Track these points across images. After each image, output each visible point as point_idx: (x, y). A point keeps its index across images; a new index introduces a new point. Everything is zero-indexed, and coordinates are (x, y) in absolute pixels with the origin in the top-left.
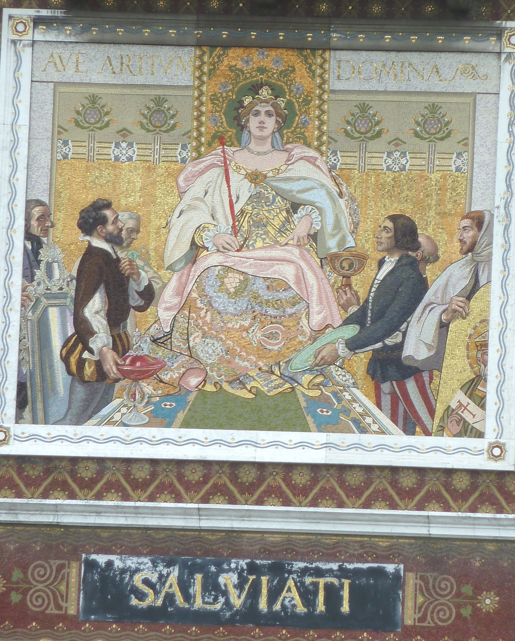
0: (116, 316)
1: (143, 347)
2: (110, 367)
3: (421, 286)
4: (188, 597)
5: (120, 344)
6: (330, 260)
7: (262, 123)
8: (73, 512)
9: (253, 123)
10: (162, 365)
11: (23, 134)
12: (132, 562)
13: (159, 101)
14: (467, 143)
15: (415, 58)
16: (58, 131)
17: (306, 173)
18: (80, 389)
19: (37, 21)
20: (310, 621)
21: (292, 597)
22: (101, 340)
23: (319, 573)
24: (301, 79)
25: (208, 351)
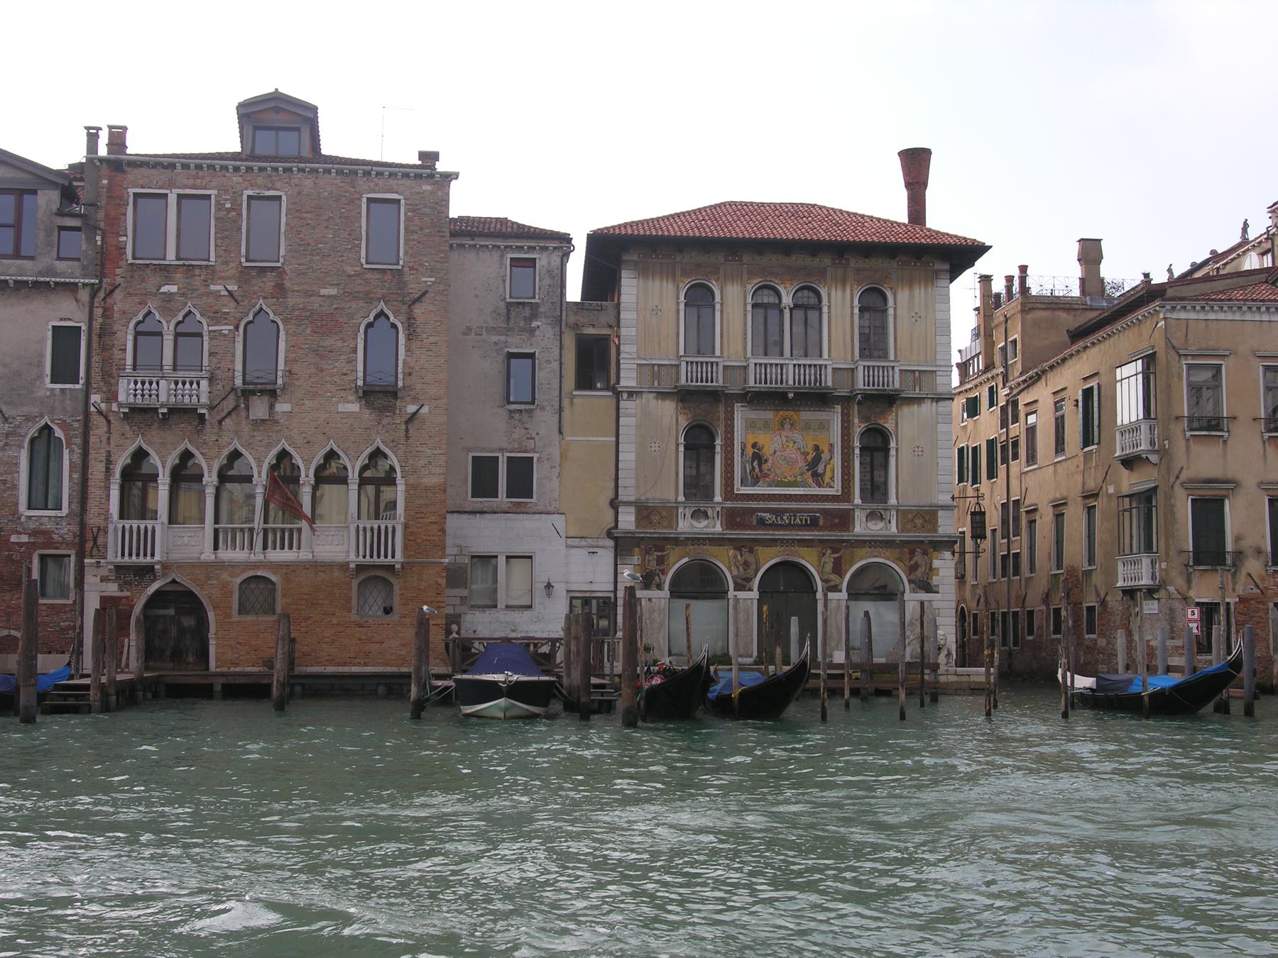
0: (760, 465)
5: (761, 471)
7: (787, 426)
8: (754, 505)
17: (797, 436)
20: (801, 525)
22: (757, 470)
25: (779, 472)
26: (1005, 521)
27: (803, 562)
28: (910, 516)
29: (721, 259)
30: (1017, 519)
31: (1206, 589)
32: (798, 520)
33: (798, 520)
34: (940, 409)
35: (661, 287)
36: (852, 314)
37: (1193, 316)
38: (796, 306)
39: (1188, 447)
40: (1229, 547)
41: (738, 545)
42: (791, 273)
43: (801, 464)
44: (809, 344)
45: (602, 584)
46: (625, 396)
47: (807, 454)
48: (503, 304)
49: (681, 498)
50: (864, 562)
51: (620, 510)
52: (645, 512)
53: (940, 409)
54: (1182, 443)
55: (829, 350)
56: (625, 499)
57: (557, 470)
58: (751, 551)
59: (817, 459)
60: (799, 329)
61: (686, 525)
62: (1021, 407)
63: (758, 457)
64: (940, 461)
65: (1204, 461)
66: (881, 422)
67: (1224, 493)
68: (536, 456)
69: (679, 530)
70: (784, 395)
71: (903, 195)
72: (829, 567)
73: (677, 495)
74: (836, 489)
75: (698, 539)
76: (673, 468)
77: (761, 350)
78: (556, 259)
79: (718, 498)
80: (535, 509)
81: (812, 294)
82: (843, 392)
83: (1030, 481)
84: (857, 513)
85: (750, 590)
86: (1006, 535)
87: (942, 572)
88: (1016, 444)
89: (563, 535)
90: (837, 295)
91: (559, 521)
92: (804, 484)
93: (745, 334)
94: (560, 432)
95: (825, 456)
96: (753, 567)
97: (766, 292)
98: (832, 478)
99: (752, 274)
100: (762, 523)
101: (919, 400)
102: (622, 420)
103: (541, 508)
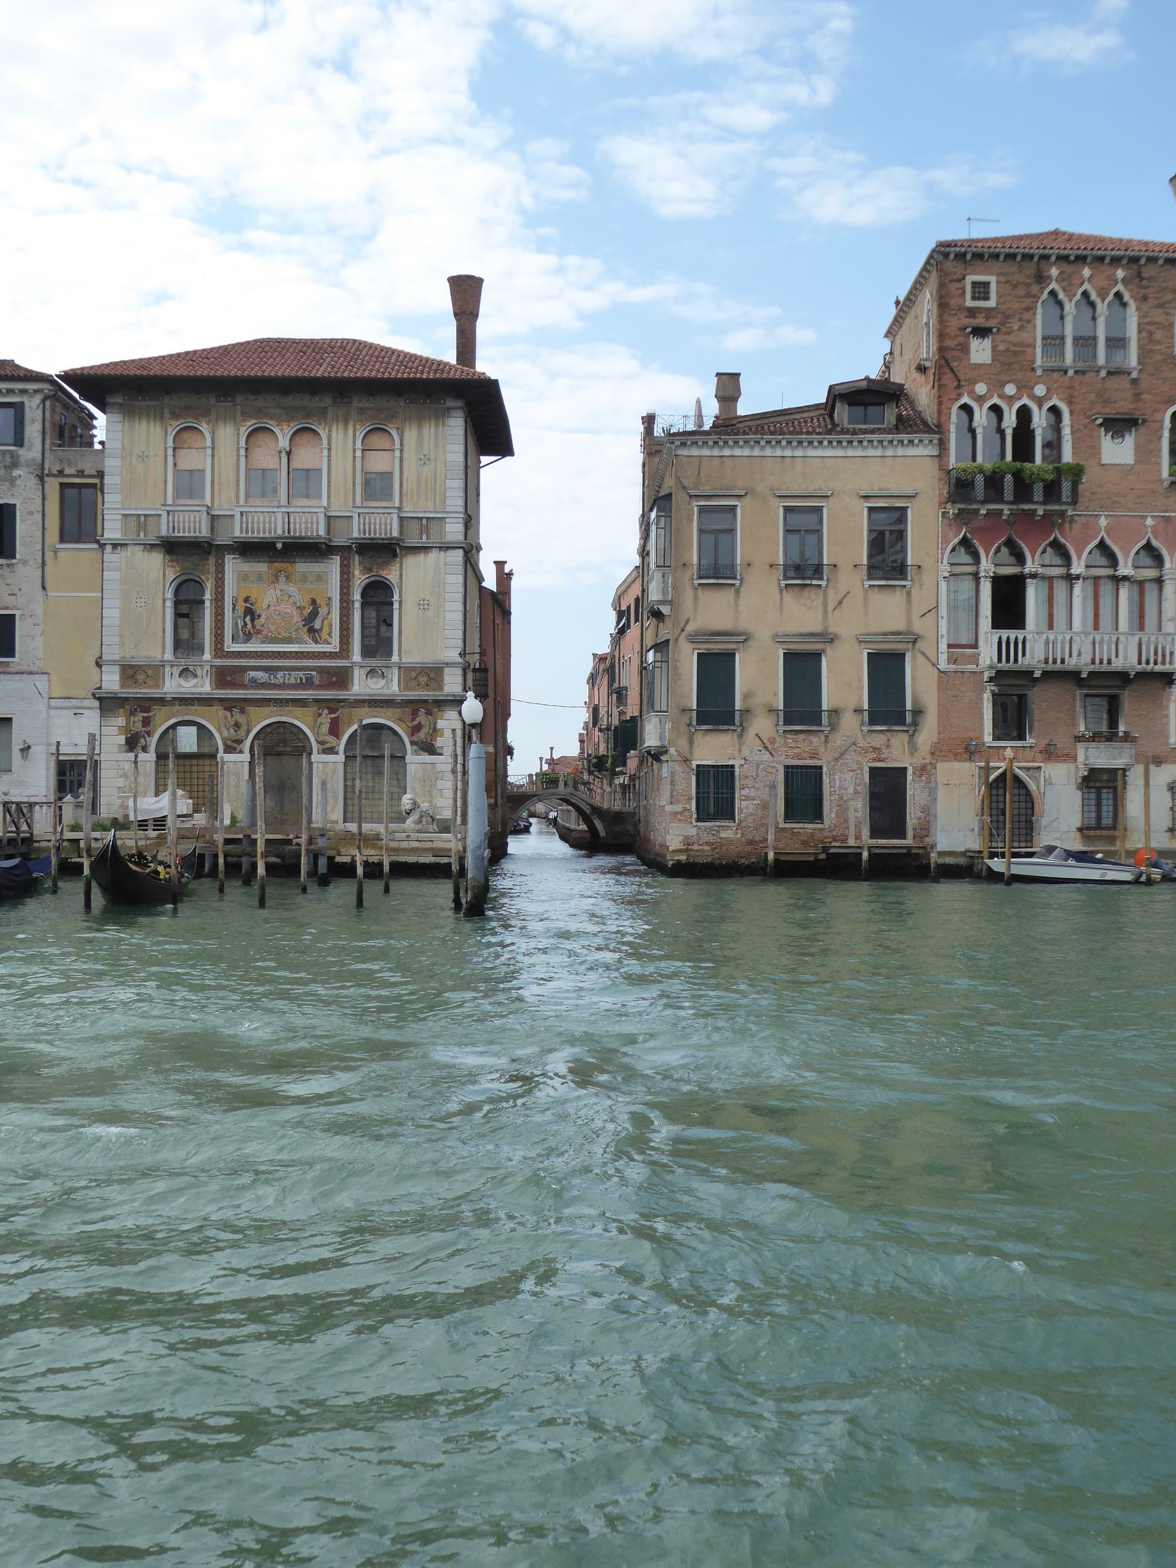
0: (252, 621)
1: (258, 627)
5: (254, 627)
7: (282, 579)
17: (292, 589)
21: (293, 681)
24: (290, 569)
25: (273, 628)
28: (414, 674)
29: (213, 400)
31: (713, 749)
34: (449, 559)
35: (148, 433)
36: (354, 457)
37: (706, 452)
39: (696, 597)
40: (909, 706)
41: (228, 704)
42: (289, 414)
43: (297, 619)
46: (109, 548)
47: (301, 608)
49: (169, 656)
52: (130, 672)
54: (689, 594)
55: (329, 496)
57: (39, 629)
58: (242, 711)
59: (314, 615)
61: (173, 685)
63: (249, 612)
65: (713, 611)
66: (384, 573)
67: (733, 646)
68: (17, 613)
69: (165, 690)
72: (325, 729)
73: (164, 653)
76: (160, 624)
79: (207, 656)
80: (17, 669)
82: (339, 541)
85: (241, 752)
89: (46, 696)
91: (41, 682)
93: (238, 481)
94: (44, 588)
95: (323, 611)
96: (244, 728)
98: (330, 634)
99: (246, 415)
100: (256, 685)
101: (425, 549)
103: (24, 668)
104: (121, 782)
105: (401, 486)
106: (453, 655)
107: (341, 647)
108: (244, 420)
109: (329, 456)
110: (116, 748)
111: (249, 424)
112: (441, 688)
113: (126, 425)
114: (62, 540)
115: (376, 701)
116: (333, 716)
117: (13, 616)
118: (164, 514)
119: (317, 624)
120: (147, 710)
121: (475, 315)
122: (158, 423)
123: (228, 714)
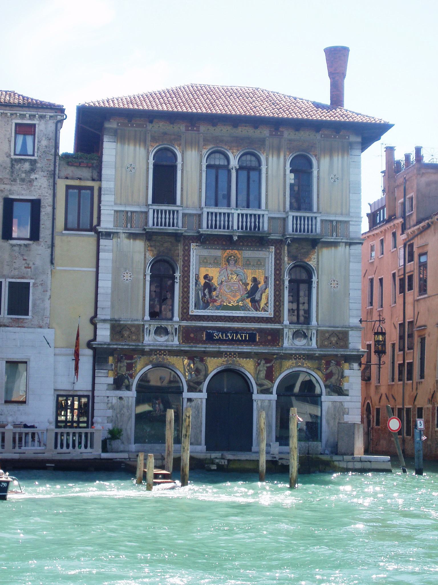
0: (210, 292)
2: (209, 301)
3: (258, 288)
4: (223, 337)
6: (243, 283)
9: (231, 262)
10: (217, 300)
11: (195, 263)
12: (214, 332)
13: (216, 258)
14: (264, 265)
15: (256, 252)
16: (200, 263)
18: (204, 305)
19: (196, 245)
20: (242, 341)
23: (243, 333)
26: (402, 338)
27: (243, 370)
28: (327, 335)
29: (183, 128)
30: (411, 336)
32: (239, 336)
33: (239, 336)
35: (135, 150)
38: (241, 168)
41: (192, 356)
42: (237, 142)
44: (251, 197)
45: (83, 384)
48: (8, 160)
49: (147, 317)
50: (291, 371)
51: (98, 326)
53: (352, 251)
56: (103, 317)
59: (255, 288)
60: (243, 185)
61: (150, 340)
62: (415, 249)
63: (209, 286)
64: (351, 292)
66: (306, 260)
68: (32, 282)
70: (231, 237)
71: (327, 81)
72: (263, 375)
73: (144, 315)
74: (270, 313)
75: (160, 350)
77: (213, 202)
78: (51, 125)
79: (176, 318)
81: (253, 158)
83: (422, 307)
84: (286, 330)
85: (201, 391)
86: (402, 349)
87: (351, 380)
88: (411, 278)
90: (273, 160)
92: (244, 308)
93: (200, 188)
94: (52, 263)
96: (203, 373)
97: (217, 155)
99: (207, 141)
101: (335, 244)
102: (101, 255)
104: (110, 413)
105: (318, 197)
106: (354, 321)
107: (275, 314)
108: (205, 145)
109: (267, 173)
110: (105, 387)
111: (209, 147)
112: (346, 346)
113: (119, 144)
114: (66, 229)
115: (300, 355)
116: (268, 365)
117: (29, 284)
118: (151, 212)
119: (257, 298)
120: (131, 358)
121: (344, 75)
122: (142, 144)
123: (191, 362)
